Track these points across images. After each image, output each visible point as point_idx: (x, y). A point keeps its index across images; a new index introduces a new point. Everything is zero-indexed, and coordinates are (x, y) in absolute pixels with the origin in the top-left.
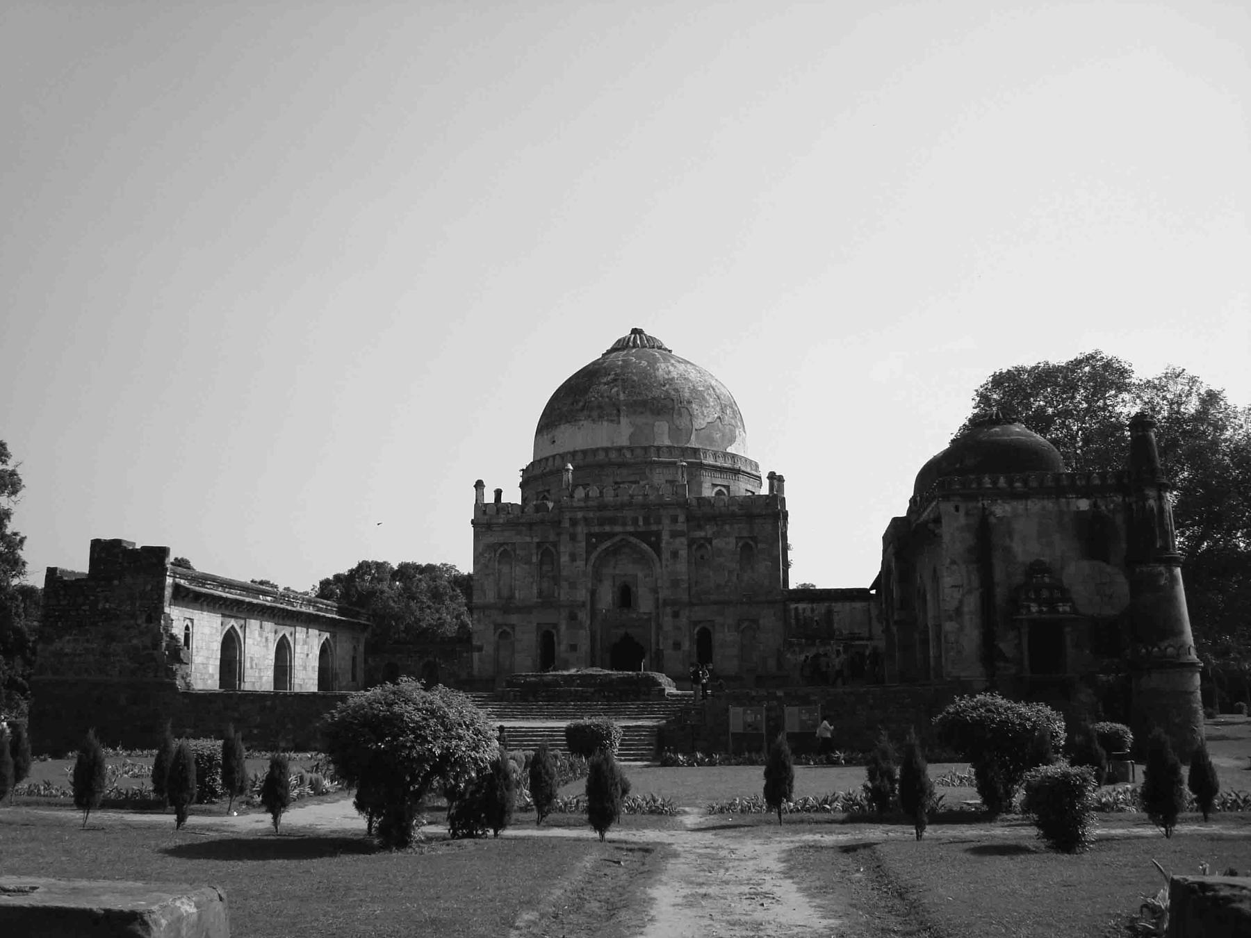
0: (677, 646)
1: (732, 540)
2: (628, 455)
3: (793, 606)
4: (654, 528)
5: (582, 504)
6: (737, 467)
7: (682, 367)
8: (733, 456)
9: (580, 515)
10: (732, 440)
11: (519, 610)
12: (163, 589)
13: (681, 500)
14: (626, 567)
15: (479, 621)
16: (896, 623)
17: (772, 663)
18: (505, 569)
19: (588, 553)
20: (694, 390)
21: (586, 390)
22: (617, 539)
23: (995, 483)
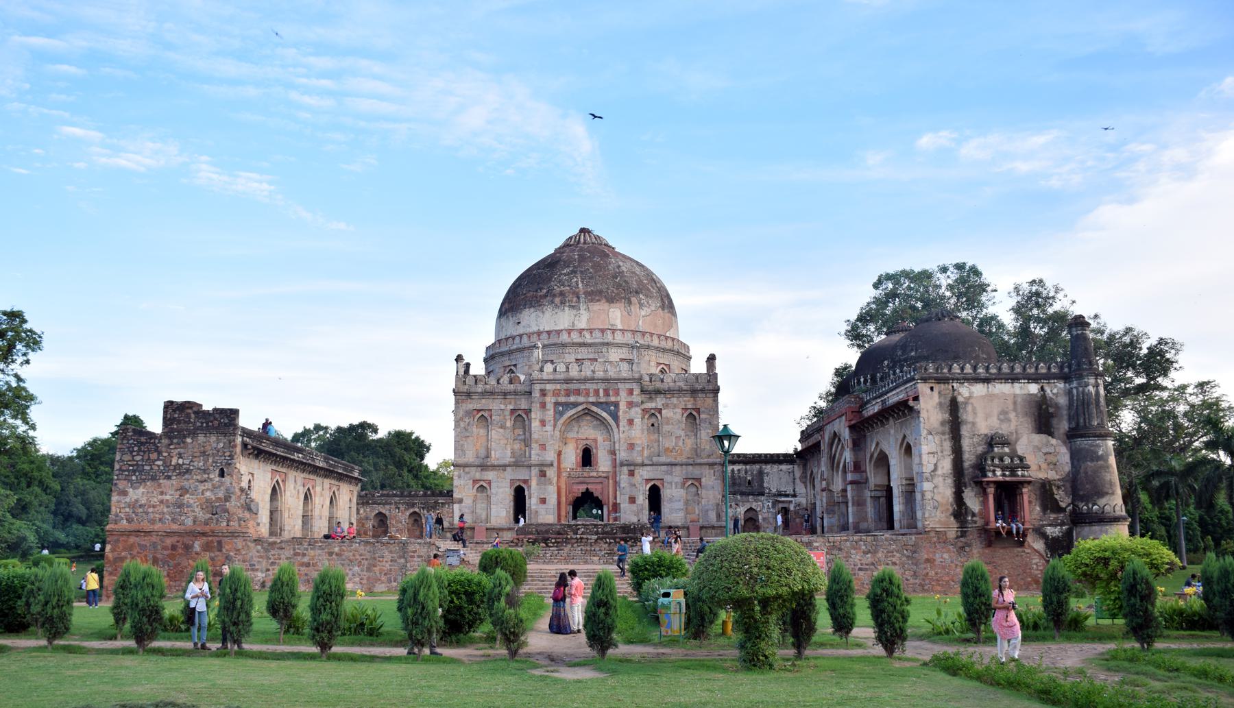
0: (632, 500)
1: (679, 411)
2: (588, 335)
3: (730, 468)
4: (613, 399)
5: (551, 377)
6: (676, 348)
7: (629, 264)
8: (673, 340)
9: (549, 387)
10: (670, 326)
11: (494, 467)
12: (235, 446)
13: (637, 376)
14: (587, 432)
15: (459, 477)
16: (852, 483)
17: (712, 516)
18: (482, 432)
19: (556, 421)
20: (640, 282)
21: (550, 280)
22: (580, 408)
23: (962, 369)
